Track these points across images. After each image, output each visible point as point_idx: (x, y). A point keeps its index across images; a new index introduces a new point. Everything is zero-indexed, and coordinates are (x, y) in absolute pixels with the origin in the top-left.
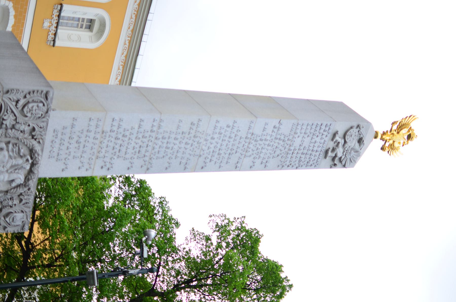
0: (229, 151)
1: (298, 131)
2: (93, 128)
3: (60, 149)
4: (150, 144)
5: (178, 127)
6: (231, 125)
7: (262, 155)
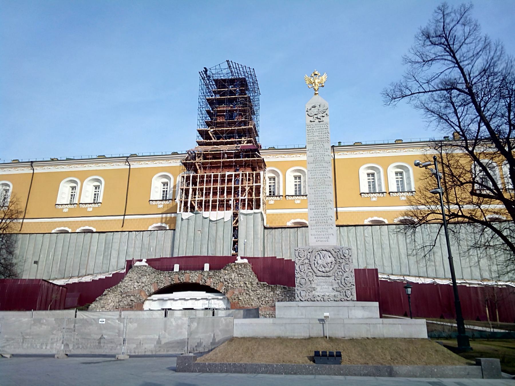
0: (322, 168)
1: (311, 140)
2: (315, 227)
3: (324, 238)
4: (320, 203)
5: (313, 194)
6: (310, 172)
7: (323, 153)
